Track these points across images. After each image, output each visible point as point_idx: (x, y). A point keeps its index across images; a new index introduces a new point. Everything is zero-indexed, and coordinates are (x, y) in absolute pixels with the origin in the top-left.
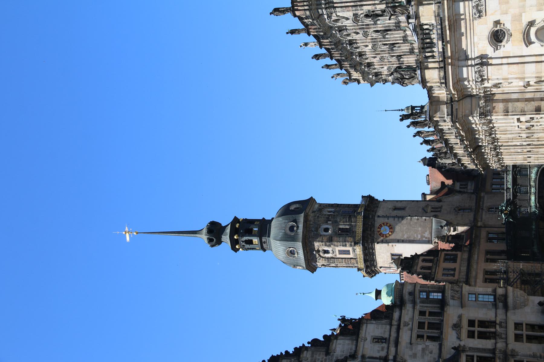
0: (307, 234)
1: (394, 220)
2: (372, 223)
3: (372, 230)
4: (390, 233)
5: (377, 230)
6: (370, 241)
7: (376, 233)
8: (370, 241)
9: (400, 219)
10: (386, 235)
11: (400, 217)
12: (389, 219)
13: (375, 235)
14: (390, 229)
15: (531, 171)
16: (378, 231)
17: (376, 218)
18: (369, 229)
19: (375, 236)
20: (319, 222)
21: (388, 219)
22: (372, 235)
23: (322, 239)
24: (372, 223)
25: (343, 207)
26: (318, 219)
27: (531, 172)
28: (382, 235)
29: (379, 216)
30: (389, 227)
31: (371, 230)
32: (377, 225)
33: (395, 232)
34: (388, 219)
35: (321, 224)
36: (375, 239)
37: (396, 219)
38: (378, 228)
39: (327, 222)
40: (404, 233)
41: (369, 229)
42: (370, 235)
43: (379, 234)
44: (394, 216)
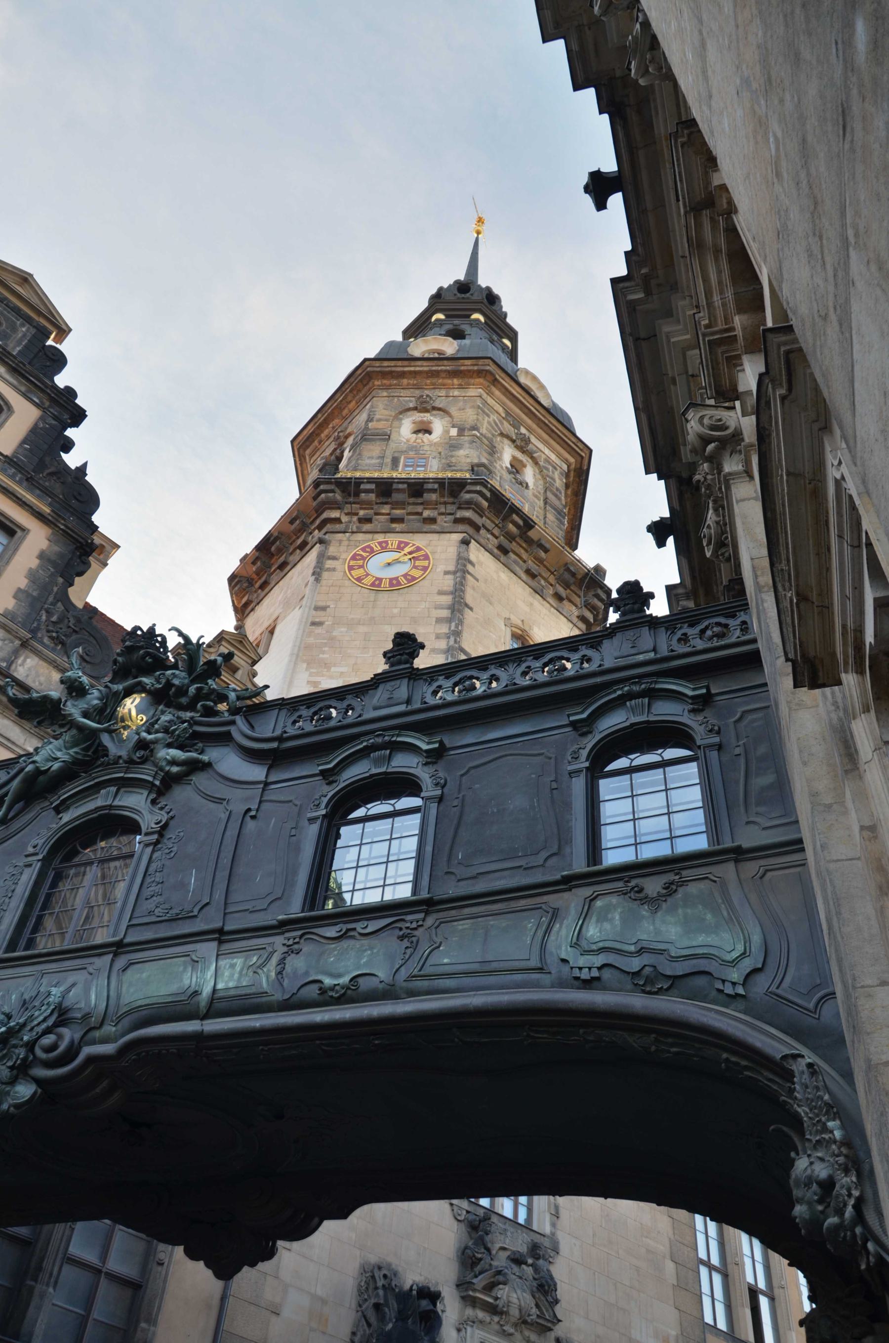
0: (405, 381)
1: (441, 593)
2: (433, 521)
3: (394, 525)
4: (368, 581)
5: (393, 540)
6: (335, 514)
7: (380, 538)
8: (335, 514)
9: (445, 613)
10: (362, 567)
11: (452, 612)
12: (451, 577)
13: (369, 536)
14: (391, 580)
15: (670, 889)
16: (387, 542)
17: (457, 537)
18: (398, 512)
19: (360, 536)
20: (460, 410)
21: (447, 573)
22: (367, 527)
23: (379, 420)
24: (433, 521)
25: (545, 518)
26: (473, 407)
27: (653, 886)
28: (364, 554)
29: (466, 542)
30: (405, 576)
31: (394, 520)
32: (419, 540)
33: (373, 594)
34: (447, 573)
35: (448, 419)
36: (347, 534)
37: (447, 600)
38: (400, 542)
39: (453, 426)
40: (362, 629)
41: (398, 512)
42: (368, 520)
43: (369, 546)
44: (463, 591)
